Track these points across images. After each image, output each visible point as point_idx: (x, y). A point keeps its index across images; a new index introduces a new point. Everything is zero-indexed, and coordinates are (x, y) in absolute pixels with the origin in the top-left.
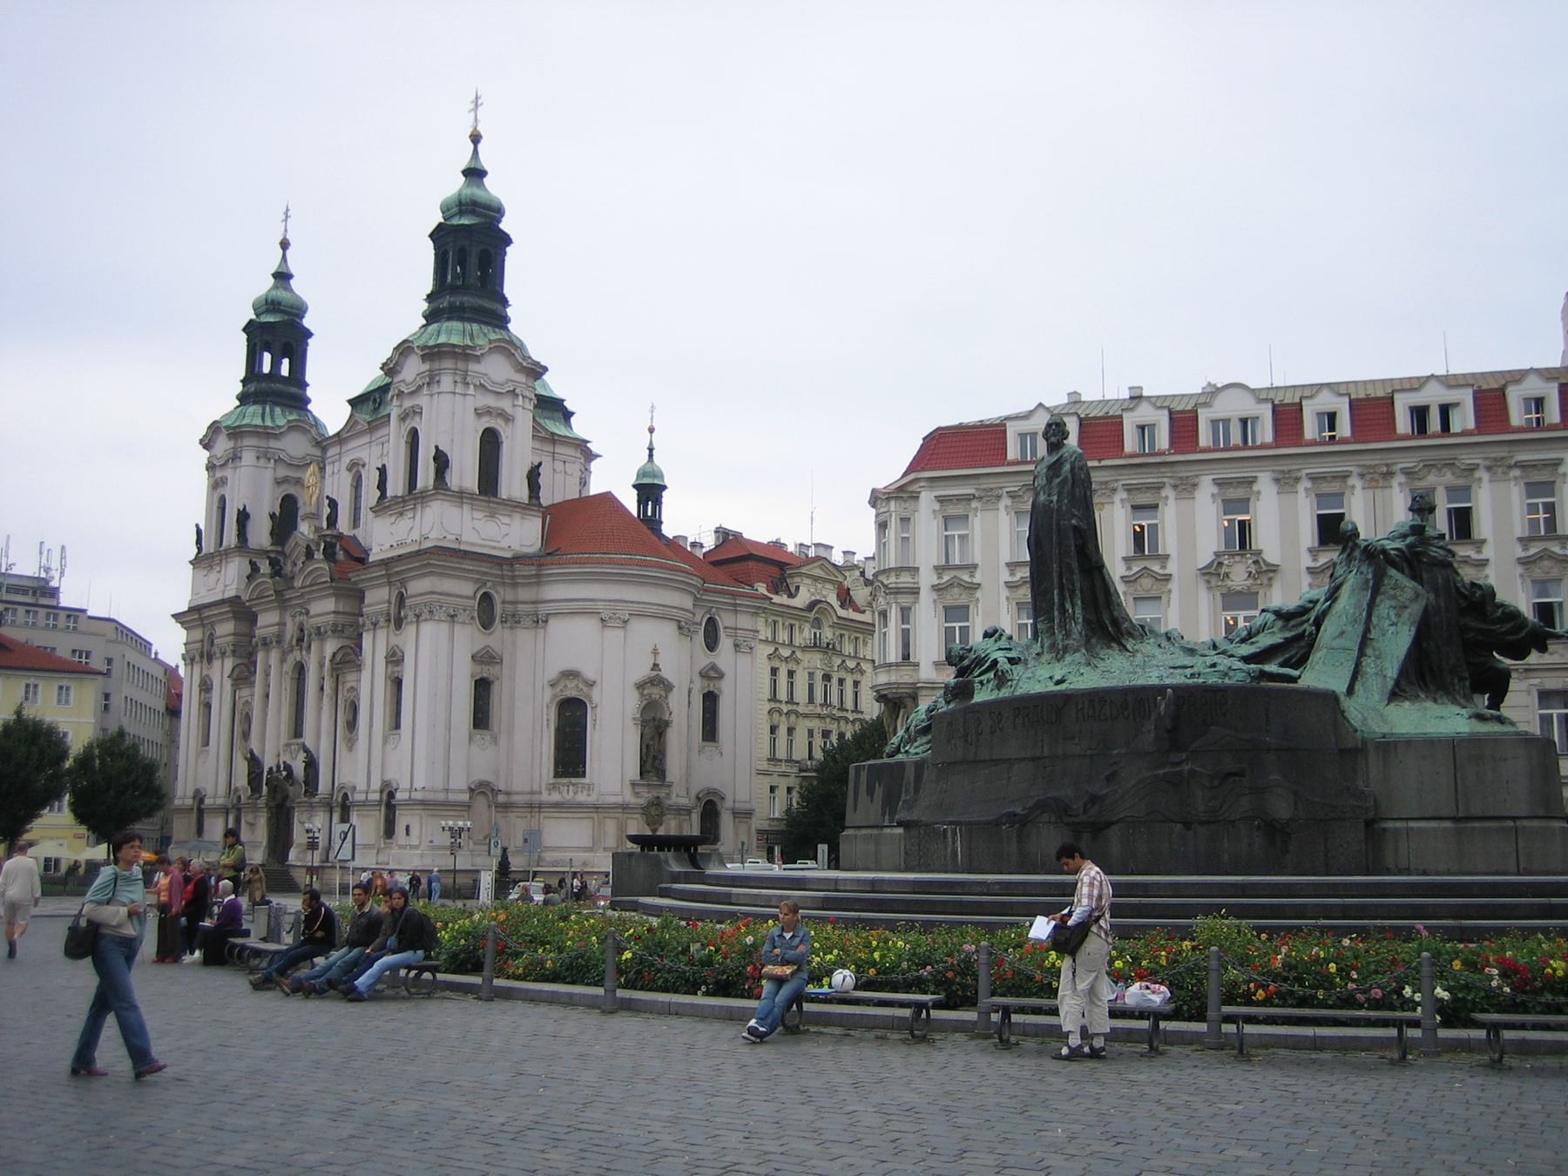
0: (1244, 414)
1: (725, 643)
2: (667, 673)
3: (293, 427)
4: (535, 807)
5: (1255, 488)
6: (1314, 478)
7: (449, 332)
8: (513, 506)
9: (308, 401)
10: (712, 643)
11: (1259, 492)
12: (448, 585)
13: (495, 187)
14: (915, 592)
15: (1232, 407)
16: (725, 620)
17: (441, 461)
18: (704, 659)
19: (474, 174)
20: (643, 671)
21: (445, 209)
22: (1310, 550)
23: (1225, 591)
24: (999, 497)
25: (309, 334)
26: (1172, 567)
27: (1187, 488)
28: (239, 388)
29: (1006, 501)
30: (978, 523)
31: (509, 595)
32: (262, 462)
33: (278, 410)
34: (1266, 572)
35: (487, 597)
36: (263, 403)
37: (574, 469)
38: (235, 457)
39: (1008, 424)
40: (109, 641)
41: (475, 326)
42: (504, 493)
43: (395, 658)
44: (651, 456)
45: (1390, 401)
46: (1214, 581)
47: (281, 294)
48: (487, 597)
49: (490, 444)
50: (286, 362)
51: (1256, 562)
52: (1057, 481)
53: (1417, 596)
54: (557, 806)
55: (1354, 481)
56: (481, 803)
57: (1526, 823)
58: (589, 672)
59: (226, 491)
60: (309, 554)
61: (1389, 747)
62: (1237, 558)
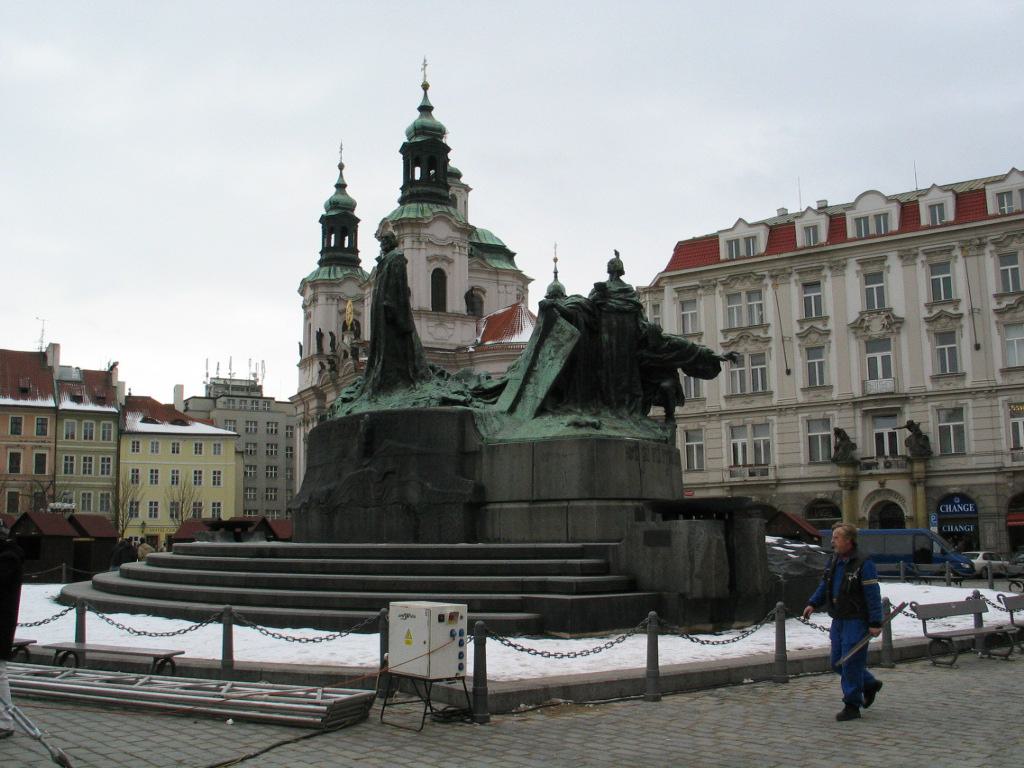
0: (878, 212)
3: (347, 278)
5: (886, 264)
7: (409, 210)
8: (457, 316)
9: (359, 261)
11: (889, 267)
13: (439, 116)
15: (869, 208)
19: (425, 109)
21: (408, 134)
22: (926, 305)
23: (867, 339)
24: (715, 286)
25: (358, 220)
26: (831, 325)
27: (839, 268)
28: (319, 257)
29: (720, 288)
30: (703, 305)
32: (330, 301)
33: (338, 269)
34: (895, 323)
36: (331, 265)
37: (513, 290)
38: (314, 300)
39: (720, 235)
40: (288, 416)
41: (425, 205)
42: (450, 308)
44: (556, 277)
45: (981, 193)
46: (860, 332)
47: (340, 197)
49: (439, 280)
50: (347, 238)
51: (888, 317)
52: (380, 275)
53: (573, 336)
55: (957, 252)
57: (576, 503)
59: (311, 320)
60: (346, 356)
61: (494, 449)
62: (875, 315)
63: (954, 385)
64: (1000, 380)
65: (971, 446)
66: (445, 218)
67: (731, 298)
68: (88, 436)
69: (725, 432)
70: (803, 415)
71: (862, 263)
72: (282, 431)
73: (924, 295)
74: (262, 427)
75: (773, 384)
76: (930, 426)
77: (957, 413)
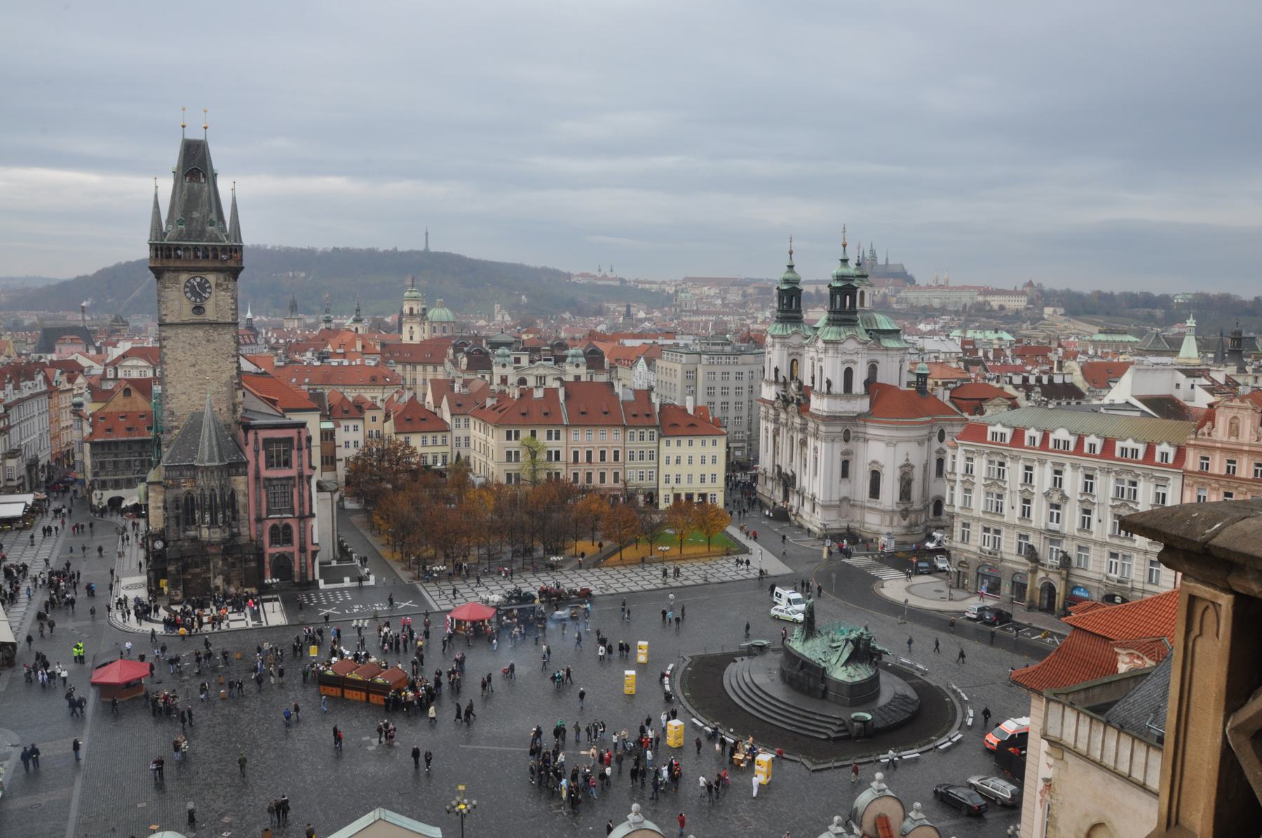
1: (948, 438)
2: (912, 462)
3: (794, 333)
4: (863, 508)
6: (1085, 468)
8: (858, 396)
10: (941, 439)
12: (831, 429)
14: (955, 481)
16: (947, 430)
17: (829, 383)
18: (936, 444)
20: (902, 462)
27: (1042, 462)
31: (856, 429)
34: (1064, 498)
35: (847, 432)
43: (816, 449)
48: (847, 432)
49: (848, 374)
54: (870, 508)
56: (845, 504)
58: (881, 462)
63: (1086, 535)
64: (1108, 540)
65: (1090, 568)
66: (852, 337)
67: (991, 462)
68: (642, 438)
69: (980, 529)
70: (1018, 531)
71: (1054, 463)
72: (746, 376)
73: (1080, 488)
74: (732, 376)
75: (1005, 511)
76: (1073, 552)
77: (1087, 549)
